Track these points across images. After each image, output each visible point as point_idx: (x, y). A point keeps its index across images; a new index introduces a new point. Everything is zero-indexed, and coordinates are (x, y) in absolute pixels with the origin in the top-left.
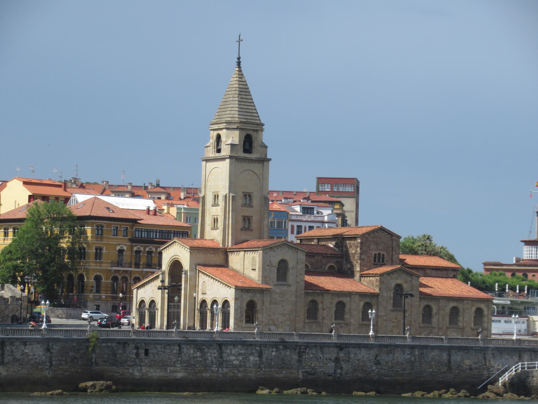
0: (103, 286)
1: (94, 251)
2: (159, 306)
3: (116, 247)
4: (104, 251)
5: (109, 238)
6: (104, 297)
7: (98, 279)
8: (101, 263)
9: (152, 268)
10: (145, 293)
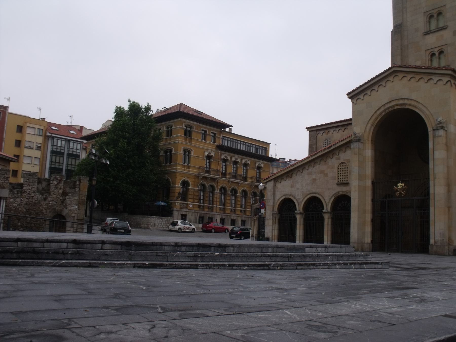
0: (190, 193)
1: (182, 152)
2: (354, 203)
3: (204, 152)
4: (193, 154)
5: (197, 141)
6: (191, 206)
7: (185, 184)
8: (189, 167)
9: (237, 179)
10: (292, 186)
